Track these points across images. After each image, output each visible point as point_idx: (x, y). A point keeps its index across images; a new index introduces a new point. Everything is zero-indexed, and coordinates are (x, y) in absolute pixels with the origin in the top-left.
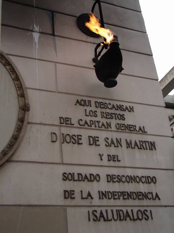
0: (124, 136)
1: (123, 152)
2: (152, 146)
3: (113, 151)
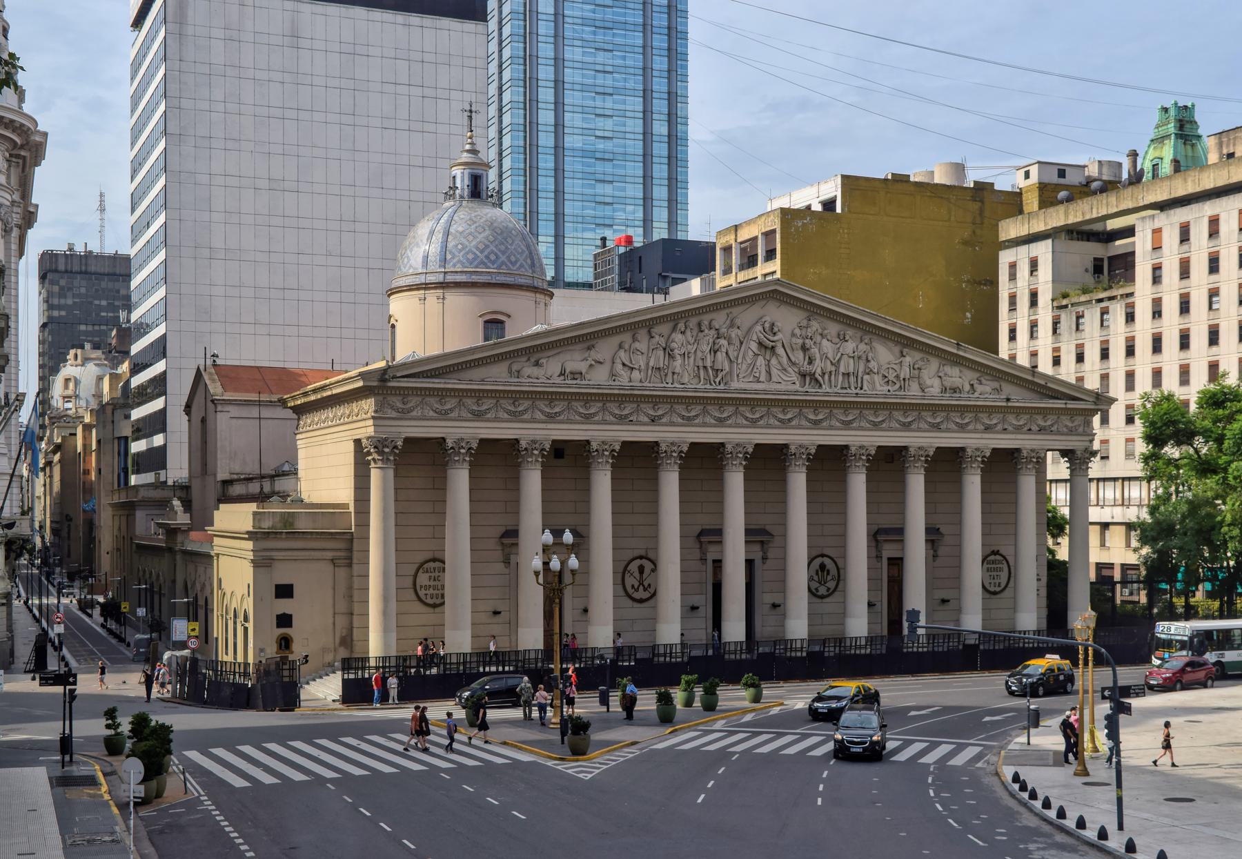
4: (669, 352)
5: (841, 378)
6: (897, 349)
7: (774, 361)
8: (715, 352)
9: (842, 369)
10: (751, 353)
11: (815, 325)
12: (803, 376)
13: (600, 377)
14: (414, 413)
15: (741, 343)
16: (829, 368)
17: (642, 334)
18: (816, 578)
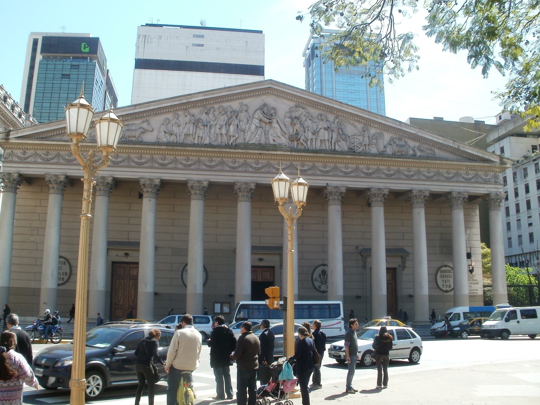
4: (197, 123)
5: (319, 143)
6: (360, 126)
7: (271, 131)
8: (229, 125)
9: (320, 138)
10: (253, 127)
11: (301, 110)
12: (292, 141)
13: (149, 137)
14: (29, 160)
15: (248, 120)
16: (310, 135)
17: (181, 113)
18: (319, 279)
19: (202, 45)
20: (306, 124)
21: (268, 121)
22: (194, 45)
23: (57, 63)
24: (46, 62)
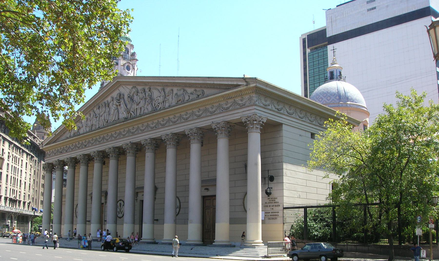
0: (275, 204)
1: (274, 208)
2: (279, 205)
3: (273, 207)
19: (375, 8)
20: (134, 100)
21: (118, 104)
22: (368, 10)
23: (319, 51)
24: (312, 54)
